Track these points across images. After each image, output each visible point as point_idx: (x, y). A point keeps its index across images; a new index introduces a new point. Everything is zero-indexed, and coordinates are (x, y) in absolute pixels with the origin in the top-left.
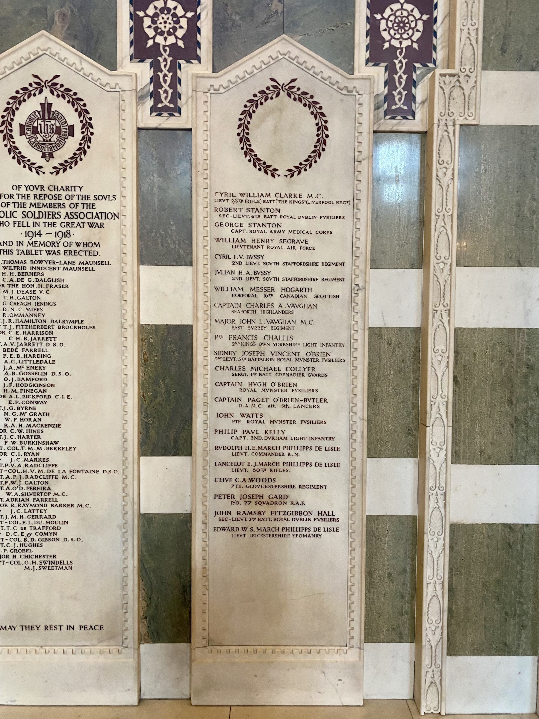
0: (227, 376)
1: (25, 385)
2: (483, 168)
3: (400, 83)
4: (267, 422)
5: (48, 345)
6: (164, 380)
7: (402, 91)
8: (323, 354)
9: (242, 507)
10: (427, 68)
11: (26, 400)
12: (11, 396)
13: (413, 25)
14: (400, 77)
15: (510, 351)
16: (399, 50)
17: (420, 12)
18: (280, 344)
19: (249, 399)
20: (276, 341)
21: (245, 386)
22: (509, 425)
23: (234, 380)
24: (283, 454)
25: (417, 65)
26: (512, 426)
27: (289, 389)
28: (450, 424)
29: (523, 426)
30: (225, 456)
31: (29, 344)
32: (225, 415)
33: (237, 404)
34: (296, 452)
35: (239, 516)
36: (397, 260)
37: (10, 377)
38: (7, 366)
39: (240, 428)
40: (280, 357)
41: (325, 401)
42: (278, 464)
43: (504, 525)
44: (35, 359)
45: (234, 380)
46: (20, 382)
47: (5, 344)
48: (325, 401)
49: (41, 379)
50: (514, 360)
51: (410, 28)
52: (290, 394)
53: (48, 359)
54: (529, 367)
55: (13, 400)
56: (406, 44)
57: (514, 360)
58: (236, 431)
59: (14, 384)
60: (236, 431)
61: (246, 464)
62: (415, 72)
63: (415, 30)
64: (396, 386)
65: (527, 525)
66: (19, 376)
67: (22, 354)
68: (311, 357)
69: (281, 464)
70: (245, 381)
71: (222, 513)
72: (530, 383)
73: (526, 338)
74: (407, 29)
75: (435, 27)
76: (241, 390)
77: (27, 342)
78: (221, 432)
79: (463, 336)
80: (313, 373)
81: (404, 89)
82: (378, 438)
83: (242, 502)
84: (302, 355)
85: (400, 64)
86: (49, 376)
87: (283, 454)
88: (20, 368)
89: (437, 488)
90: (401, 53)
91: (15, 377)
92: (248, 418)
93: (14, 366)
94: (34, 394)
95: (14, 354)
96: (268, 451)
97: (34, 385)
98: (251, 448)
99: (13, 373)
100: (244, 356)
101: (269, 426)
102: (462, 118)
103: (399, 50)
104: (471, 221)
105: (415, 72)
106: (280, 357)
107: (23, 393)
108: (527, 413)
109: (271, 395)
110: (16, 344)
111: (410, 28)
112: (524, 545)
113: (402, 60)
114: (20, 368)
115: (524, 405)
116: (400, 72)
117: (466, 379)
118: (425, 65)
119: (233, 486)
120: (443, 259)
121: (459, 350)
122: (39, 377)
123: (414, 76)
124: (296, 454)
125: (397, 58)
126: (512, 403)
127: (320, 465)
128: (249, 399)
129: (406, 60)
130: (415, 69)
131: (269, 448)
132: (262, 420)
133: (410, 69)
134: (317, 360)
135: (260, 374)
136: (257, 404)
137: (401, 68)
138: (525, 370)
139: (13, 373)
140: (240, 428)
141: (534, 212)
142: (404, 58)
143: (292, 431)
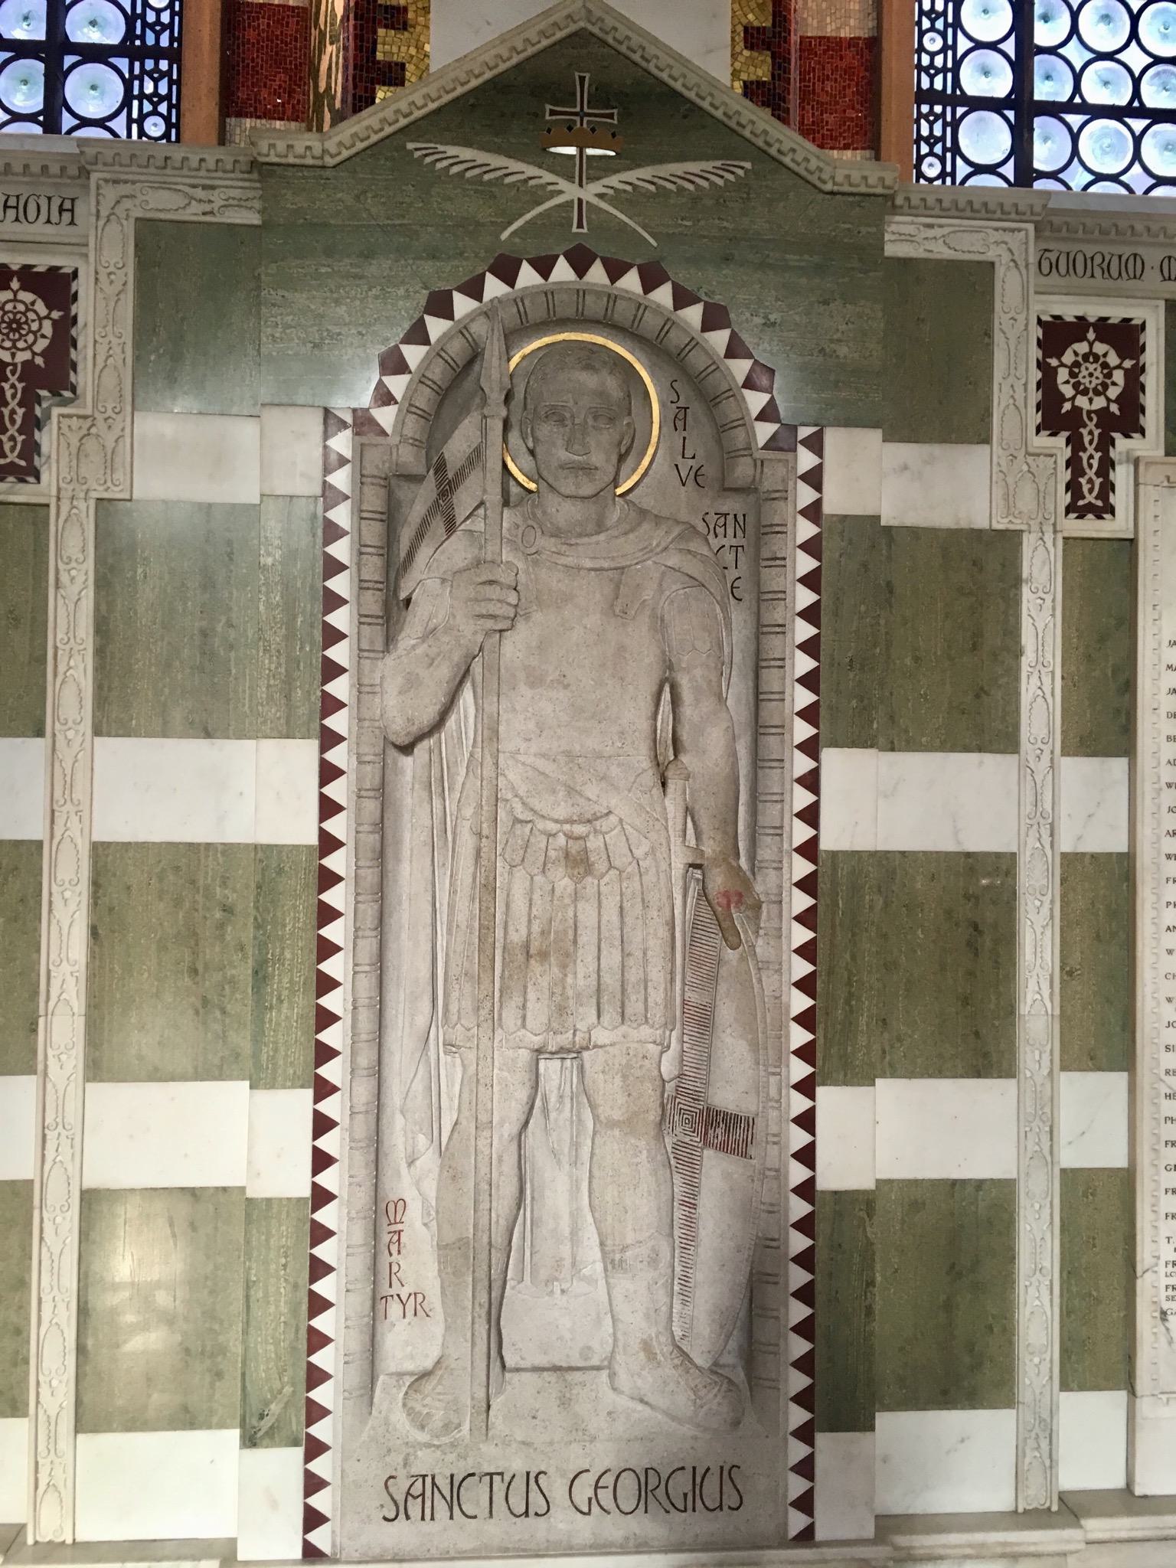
2: (140, 571)
3: (13, 421)
7: (16, 434)
10: (58, 399)
13: (35, 326)
14: (13, 412)
15: (193, 882)
16: (11, 367)
17: (47, 306)
22: (191, 1012)
25: (44, 393)
26: (197, 1013)
29: (218, 1014)
36: (11, 721)
50: (199, 898)
51: (30, 331)
54: (228, 910)
56: (22, 357)
57: (199, 898)
62: (40, 405)
63: (38, 334)
64: (10, 944)
65: (225, 1189)
72: (228, 938)
73: (221, 860)
74: (23, 332)
75: (73, 332)
79: (107, 856)
81: (20, 431)
85: (13, 391)
89: (60, 1127)
90: (13, 373)
102: (101, 488)
103: (11, 367)
104: (121, 659)
105: (40, 405)
108: (224, 988)
111: (30, 331)
112: (220, 1224)
113: (17, 383)
115: (217, 977)
116: (13, 404)
117: (113, 932)
118: (55, 393)
120: (70, 724)
121: (102, 880)
123: (38, 411)
125: (6, 380)
126: (195, 971)
129: (23, 384)
130: (39, 400)
133: (29, 400)
137: (14, 396)
138: (218, 915)
141: (231, 647)
142: (20, 380)
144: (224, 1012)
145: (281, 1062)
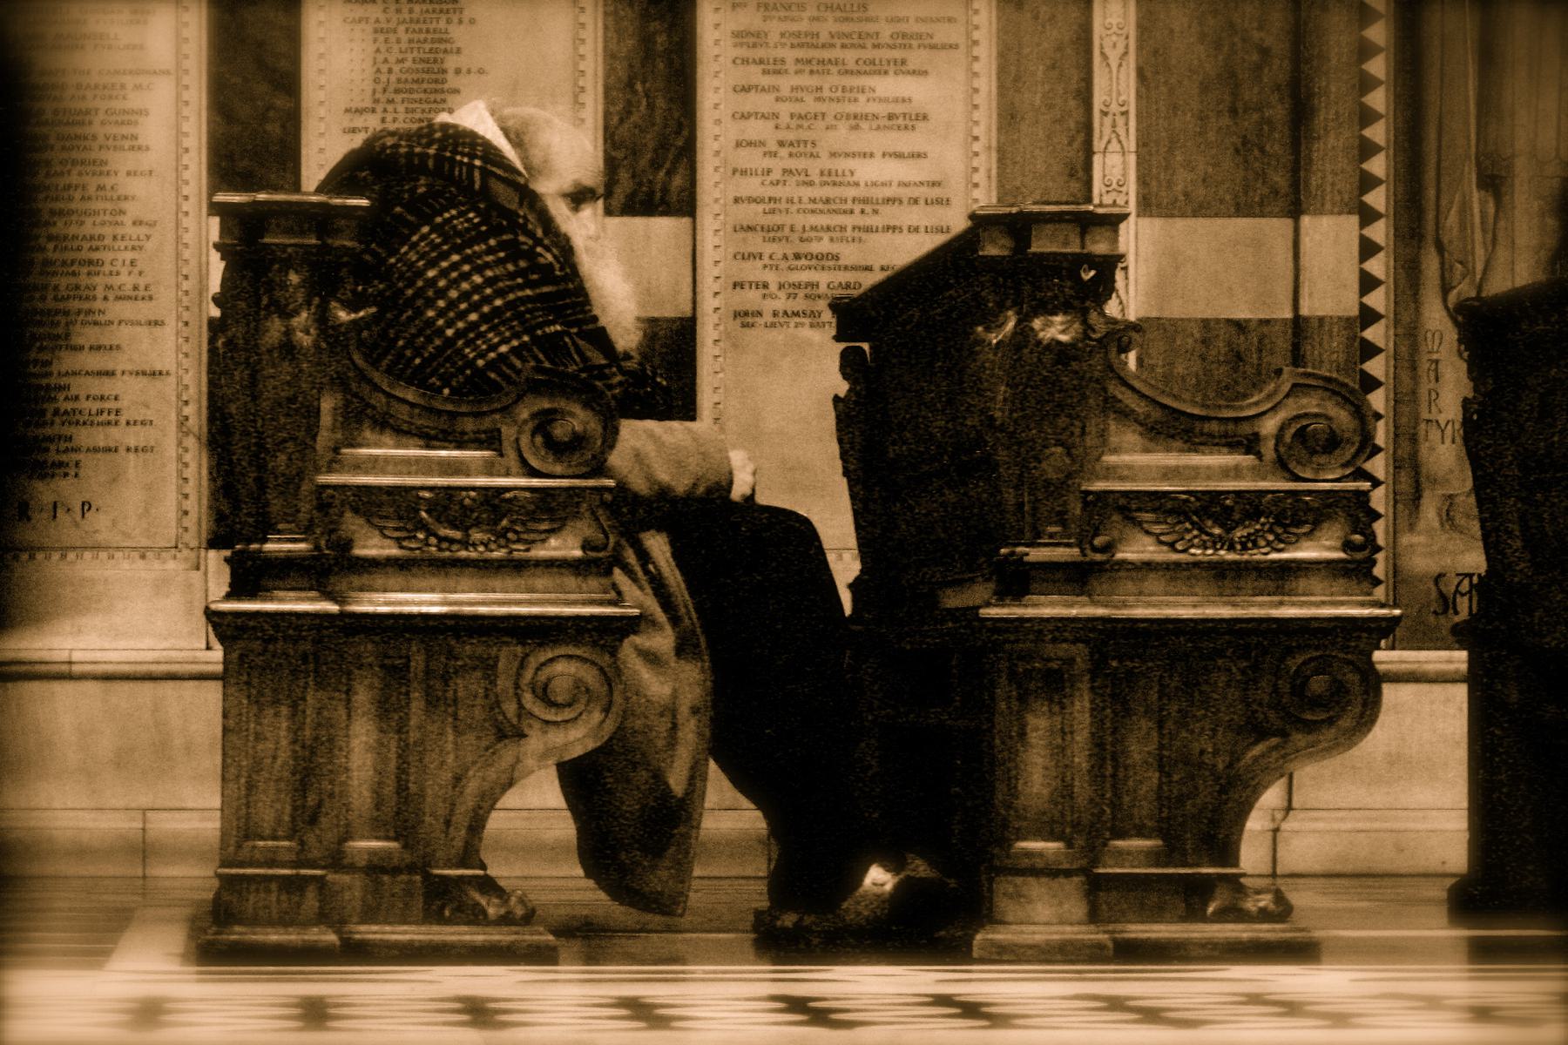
0: (755, 75)
1: (411, 91)
4: (824, 155)
5: (449, 21)
6: (644, 82)
8: (920, 36)
9: (781, 303)
11: (410, 116)
12: (385, 110)
18: (846, 19)
19: (792, 116)
20: (838, 14)
21: (785, 92)
22: (1232, 150)
23: (766, 81)
24: (852, 212)
26: (1237, 151)
27: (862, 98)
28: (1133, 147)
29: (1256, 152)
30: (752, 214)
31: (418, 22)
32: (750, 144)
33: (771, 124)
34: (876, 207)
35: (776, 320)
37: (384, 78)
38: (380, 58)
39: (777, 165)
40: (846, 41)
41: (925, 117)
42: (843, 228)
43: (1229, 321)
44: (427, 46)
45: (766, 81)
46: (401, 86)
47: (377, 21)
48: (925, 117)
49: (436, 81)
52: (862, 106)
53: (448, 46)
55: (389, 118)
58: (769, 171)
59: (391, 88)
60: (769, 171)
61: (787, 230)
66: (400, 75)
67: (405, 37)
68: (899, 41)
69: (849, 229)
70: (785, 83)
71: (746, 314)
76: (777, 99)
77: (414, 16)
78: (744, 172)
80: (903, 68)
82: (1018, 183)
83: (782, 294)
84: (885, 37)
86: (450, 76)
87: (852, 212)
88: (402, 61)
91: (393, 78)
92: (791, 149)
93: (392, 59)
94: (425, 106)
95: (392, 37)
96: (826, 207)
97: (425, 91)
98: (796, 200)
99: (390, 71)
100: (784, 40)
101: (825, 163)
106: (846, 41)
107: (406, 105)
109: (832, 109)
110: (394, 19)
114: (402, 61)
115: (1255, 116)
119: (765, 266)
122: (434, 76)
124: (876, 212)
127: (917, 230)
128: (792, 116)
131: (828, 201)
132: (814, 151)
134: (910, 46)
135: (812, 72)
136: (806, 124)
139: (390, 71)
140: (777, 165)
143: (866, 171)
144: (1262, 150)
145: (1329, 190)
